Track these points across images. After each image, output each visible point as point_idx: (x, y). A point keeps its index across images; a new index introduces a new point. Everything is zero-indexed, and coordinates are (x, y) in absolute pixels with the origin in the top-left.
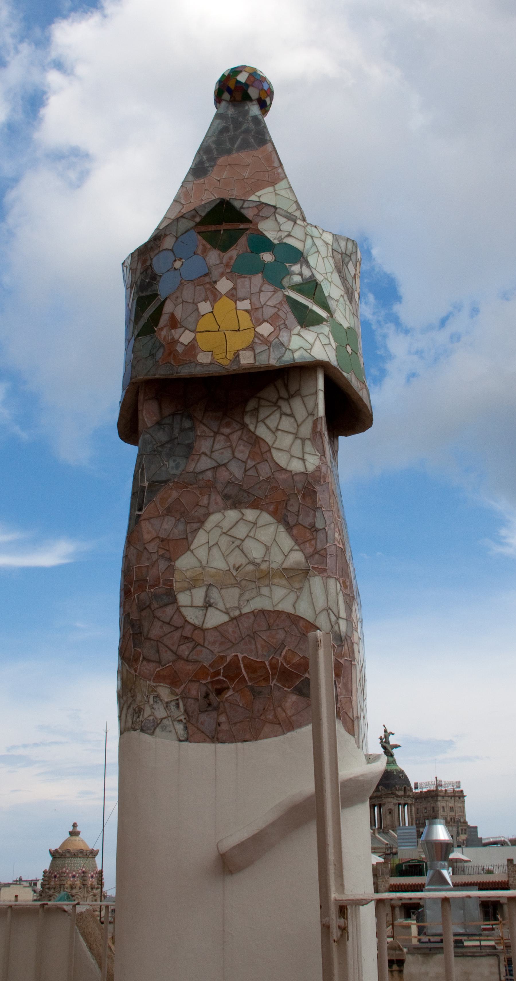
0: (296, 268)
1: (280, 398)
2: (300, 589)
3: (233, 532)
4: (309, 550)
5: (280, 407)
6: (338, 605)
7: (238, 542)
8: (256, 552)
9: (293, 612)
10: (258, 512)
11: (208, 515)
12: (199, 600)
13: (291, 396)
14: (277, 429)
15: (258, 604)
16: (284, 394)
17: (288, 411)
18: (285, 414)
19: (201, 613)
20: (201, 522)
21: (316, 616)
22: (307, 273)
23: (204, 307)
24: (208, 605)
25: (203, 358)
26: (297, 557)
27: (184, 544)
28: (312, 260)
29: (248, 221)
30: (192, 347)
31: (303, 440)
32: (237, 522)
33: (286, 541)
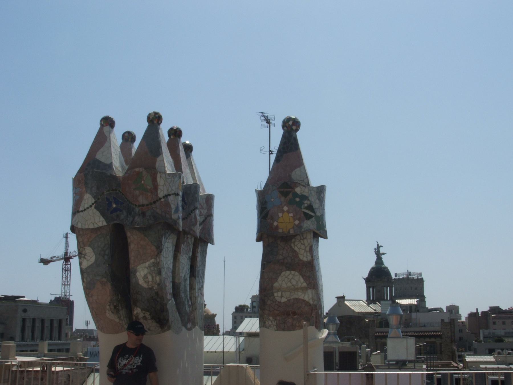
0: (306, 202)
1: (301, 239)
8: (294, 283)
11: (281, 272)
12: (280, 295)
13: (304, 239)
15: (295, 296)
16: (302, 238)
17: (303, 243)
22: (309, 203)
23: (280, 215)
24: (282, 296)
25: (280, 231)
26: (305, 284)
27: (276, 280)
28: (310, 198)
30: (277, 227)
31: (307, 252)
33: (302, 280)
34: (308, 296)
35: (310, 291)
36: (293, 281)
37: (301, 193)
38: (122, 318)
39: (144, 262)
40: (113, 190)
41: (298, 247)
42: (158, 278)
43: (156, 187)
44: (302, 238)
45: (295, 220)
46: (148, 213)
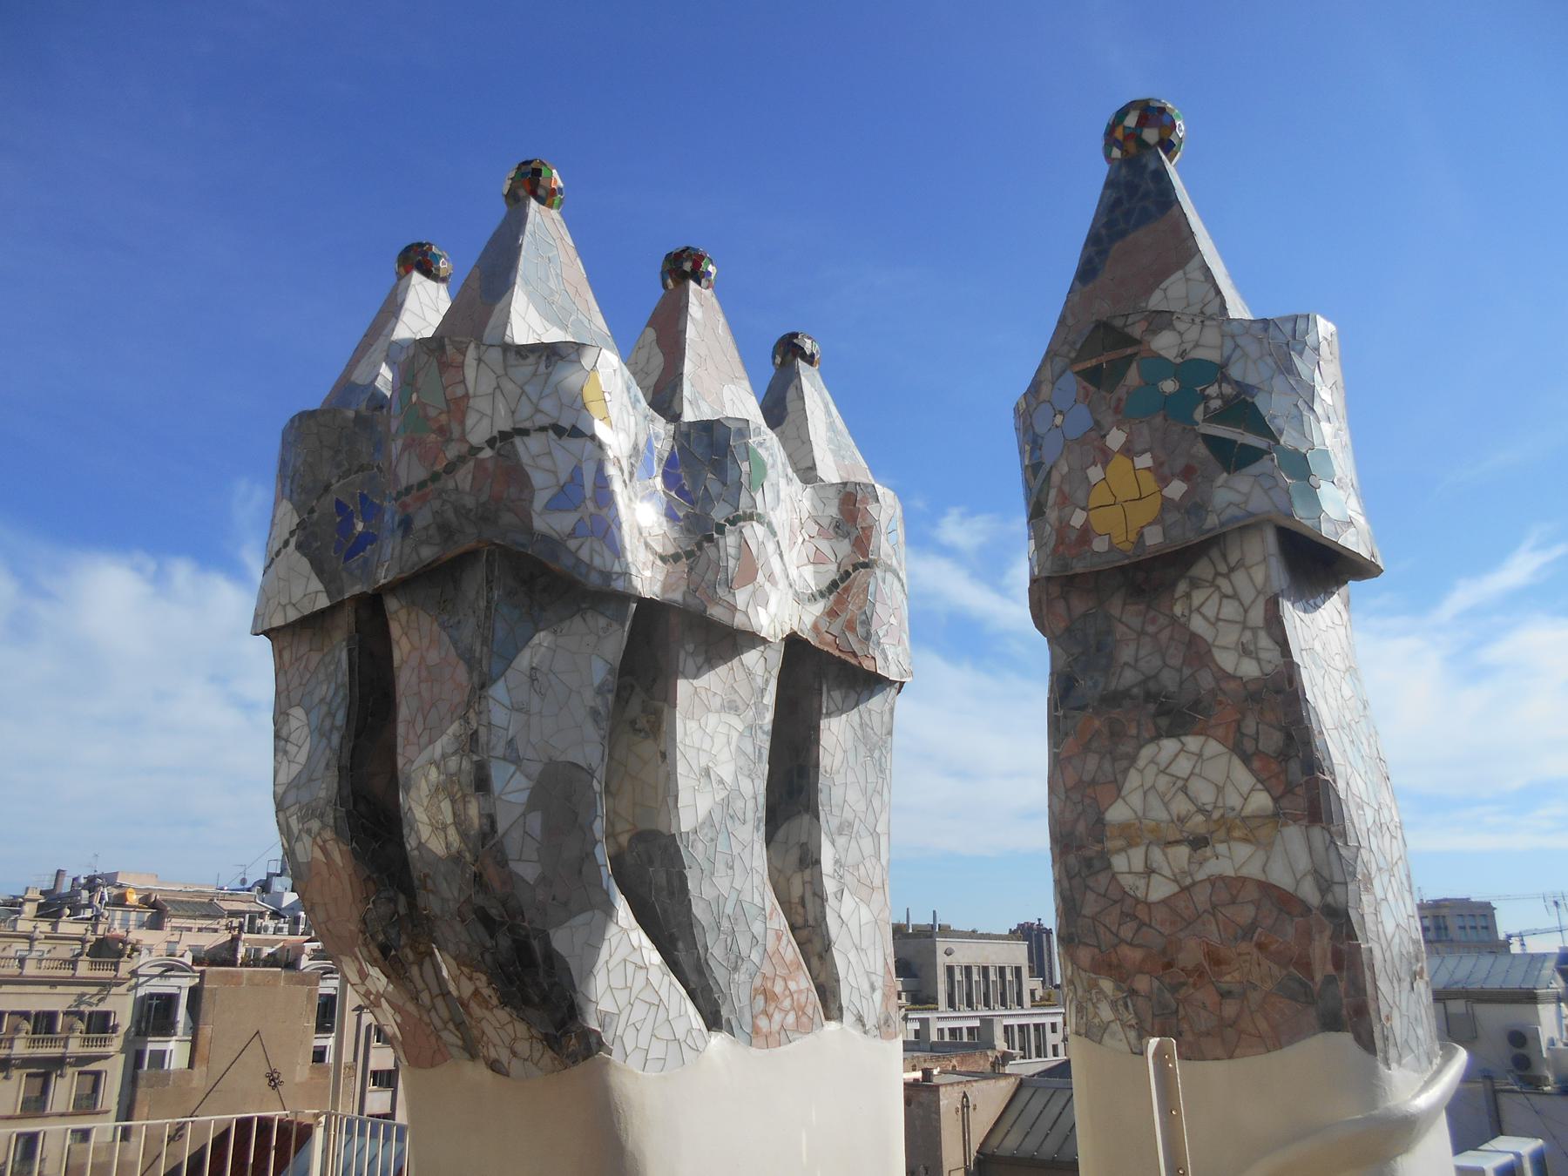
0: (1213, 390)
1: (1217, 574)
2: (1272, 844)
3: (1173, 769)
4: (1279, 791)
5: (1218, 588)
6: (1329, 864)
7: (1180, 783)
8: (1206, 796)
9: (1263, 878)
10: (1202, 738)
12: (1139, 866)
13: (1232, 570)
14: (1218, 619)
15: (1214, 867)
16: (1223, 568)
17: (1229, 591)
18: (1227, 597)
19: (1141, 883)
20: (1133, 759)
21: (1298, 882)
23: (1095, 473)
24: (1149, 871)
25: (1099, 545)
26: (1261, 801)
28: (1235, 372)
29: (1137, 342)
32: (1176, 756)
34: (1287, 861)
35: (1293, 834)
36: (1196, 786)
37: (1183, 354)
38: (425, 997)
39: (431, 742)
40: (361, 468)
41: (1212, 613)
42: (473, 810)
43: (459, 406)
44: (1223, 568)
45: (1164, 481)
46: (423, 518)
